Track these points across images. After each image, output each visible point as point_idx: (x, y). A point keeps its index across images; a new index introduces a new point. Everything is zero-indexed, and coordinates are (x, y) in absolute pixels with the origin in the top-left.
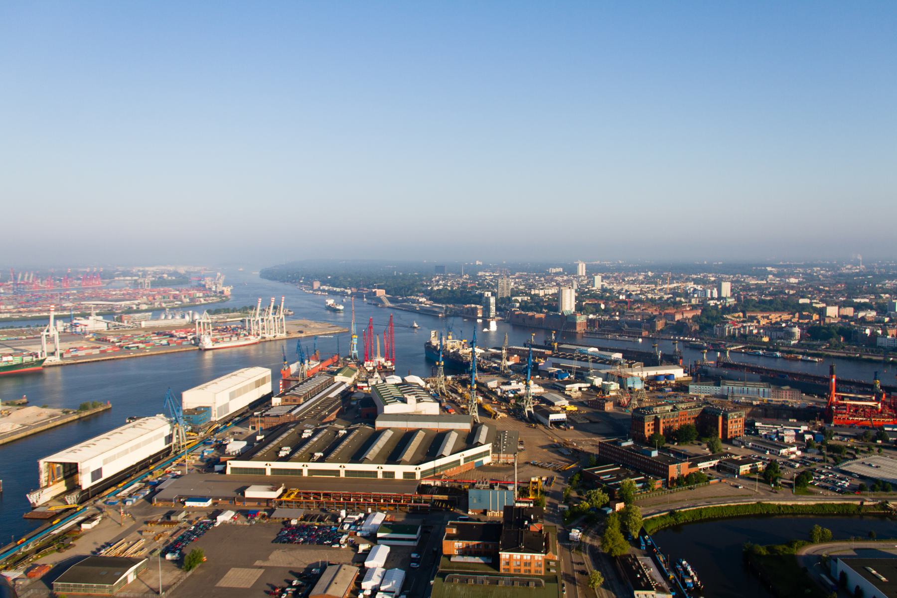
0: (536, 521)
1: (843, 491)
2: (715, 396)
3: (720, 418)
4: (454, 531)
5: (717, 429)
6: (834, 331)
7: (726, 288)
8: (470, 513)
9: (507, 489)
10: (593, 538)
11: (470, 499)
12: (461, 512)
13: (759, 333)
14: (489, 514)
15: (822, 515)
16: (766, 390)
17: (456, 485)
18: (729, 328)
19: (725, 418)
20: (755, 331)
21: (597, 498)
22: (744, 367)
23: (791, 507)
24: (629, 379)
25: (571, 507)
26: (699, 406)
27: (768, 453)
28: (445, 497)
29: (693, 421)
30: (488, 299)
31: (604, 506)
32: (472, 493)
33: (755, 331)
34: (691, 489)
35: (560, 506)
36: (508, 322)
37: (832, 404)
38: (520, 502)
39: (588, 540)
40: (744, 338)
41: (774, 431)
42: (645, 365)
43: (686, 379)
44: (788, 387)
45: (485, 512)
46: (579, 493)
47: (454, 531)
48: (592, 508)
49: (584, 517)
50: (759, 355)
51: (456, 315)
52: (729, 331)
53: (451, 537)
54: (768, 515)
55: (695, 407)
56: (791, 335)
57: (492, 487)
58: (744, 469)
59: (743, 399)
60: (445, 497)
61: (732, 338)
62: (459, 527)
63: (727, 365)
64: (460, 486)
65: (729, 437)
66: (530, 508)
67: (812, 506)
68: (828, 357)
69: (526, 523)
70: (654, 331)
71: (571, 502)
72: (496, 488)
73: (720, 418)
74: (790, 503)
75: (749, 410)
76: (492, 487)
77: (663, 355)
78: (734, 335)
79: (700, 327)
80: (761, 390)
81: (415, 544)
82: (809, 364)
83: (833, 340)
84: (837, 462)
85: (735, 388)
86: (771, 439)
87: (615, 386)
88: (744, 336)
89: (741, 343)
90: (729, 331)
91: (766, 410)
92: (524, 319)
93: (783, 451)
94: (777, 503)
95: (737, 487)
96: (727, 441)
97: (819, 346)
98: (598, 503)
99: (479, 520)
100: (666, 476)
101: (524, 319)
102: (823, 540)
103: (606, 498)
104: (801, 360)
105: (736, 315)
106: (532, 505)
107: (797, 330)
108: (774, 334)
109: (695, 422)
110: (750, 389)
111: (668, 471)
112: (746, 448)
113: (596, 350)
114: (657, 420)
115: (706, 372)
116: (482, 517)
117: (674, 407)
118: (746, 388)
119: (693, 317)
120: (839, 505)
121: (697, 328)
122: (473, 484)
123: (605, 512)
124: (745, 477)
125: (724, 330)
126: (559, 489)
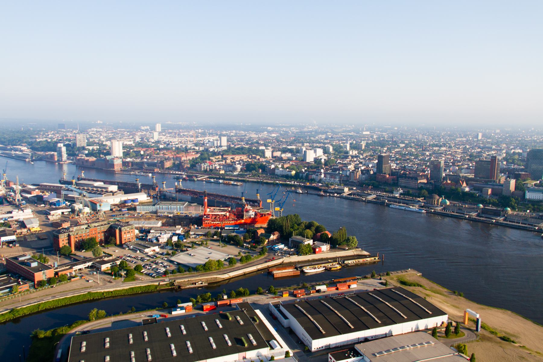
1: (159, 274)
2: (150, 213)
3: (117, 231)
5: (116, 238)
6: (257, 167)
7: (224, 140)
13: (220, 168)
15: (133, 294)
16: (181, 207)
18: (205, 166)
19: (120, 231)
20: (218, 167)
22: (188, 191)
23: (112, 292)
24: (98, 205)
26: (109, 224)
27: (138, 252)
29: (103, 234)
30: (60, 148)
33: (218, 167)
34: (52, 287)
36: (74, 164)
37: (205, 215)
40: (211, 172)
41: (158, 235)
42: (125, 193)
43: (149, 201)
44: (196, 204)
50: (211, 182)
51: (40, 159)
52: (204, 168)
54: (94, 300)
55: (105, 224)
56: (235, 169)
58: (104, 267)
59: (166, 214)
61: (205, 172)
63: (179, 191)
65: (123, 242)
67: (126, 290)
68: (248, 181)
70: (163, 168)
73: (117, 231)
74: (112, 290)
75: (164, 221)
77: (143, 186)
78: (207, 169)
79: (191, 165)
80: (178, 207)
82: (236, 187)
83: (254, 172)
84: (173, 254)
85: (164, 206)
86: (152, 241)
87: (87, 210)
88: (211, 170)
89: (208, 175)
90: (204, 168)
91: (174, 220)
92: (83, 162)
93: (147, 250)
94: (102, 291)
95: (88, 281)
96: (121, 246)
97: (246, 175)
100: (33, 281)
101: (83, 162)
102: (98, 318)
104: (232, 185)
105: (217, 157)
107: (239, 167)
108: (228, 168)
109: (105, 235)
110: (172, 206)
111: (34, 277)
112: (129, 249)
113: (102, 183)
114: (69, 236)
115: (165, 195)
117: (89, 226)
118: (170, 206)
119: (193, 159)
120: (144, 287)
121: (189, 166)
124: (105, 273)
125: (201, 167)
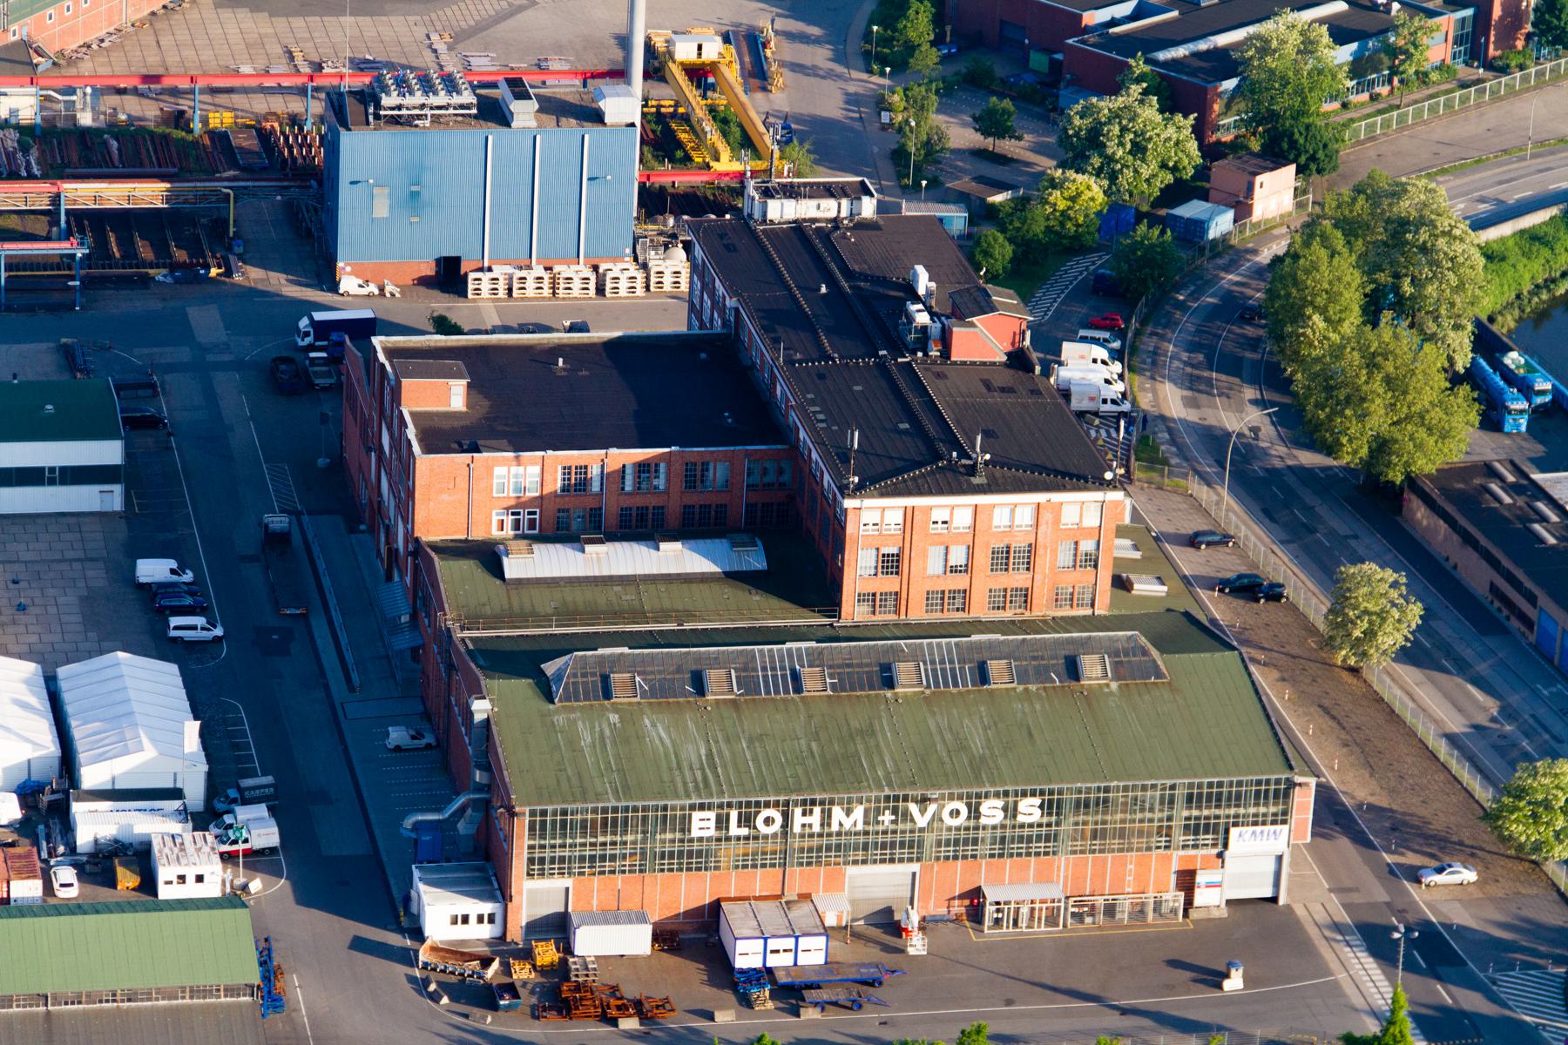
0: (965, 304)
4: (454, 396)
8: (349, 284)
9: (597, 117)
10: (1193, 384)
11: (346, 195)
12: (280, 284)
14: (481, 286)
17: (148, 111)
21: (1138, 149)
25: (982, 214)
28: (149, 193)
31: (1179, 192)
32: (362, 153)
35: (909, 209)
38: (791, 192)
39: (1170, 400)
45: (450, 276)
46: (991, 124)
47: (454, 396)
48: (1117, 216)
49: (1079, 269)
53: (446, 436)
57: (492, 112)
60: (149, 193)
62: (481, 365)
64: (179, 119)
66: (863, 226)
69: (923, 318)
71: (964, 184)
72: (524, 113)
76: (492, 112)
81: (111, 498)
98: (1147, 178)
99: (443, 325)
103: (1175, 138)
106: (868, 208)
116: (442, 304)
122: (368, 97)
123: (1199, 226)
126: (828, 102)
